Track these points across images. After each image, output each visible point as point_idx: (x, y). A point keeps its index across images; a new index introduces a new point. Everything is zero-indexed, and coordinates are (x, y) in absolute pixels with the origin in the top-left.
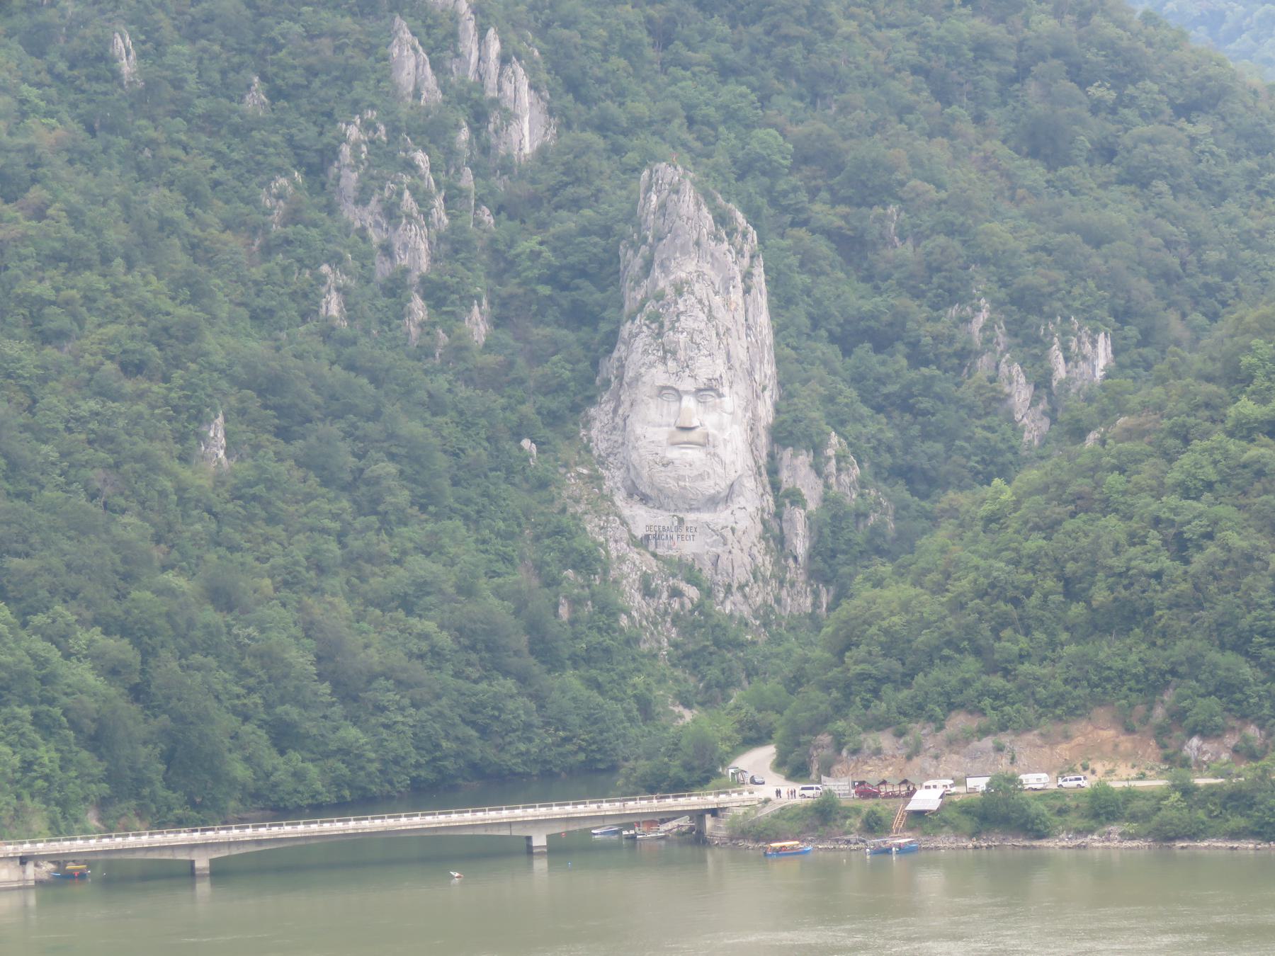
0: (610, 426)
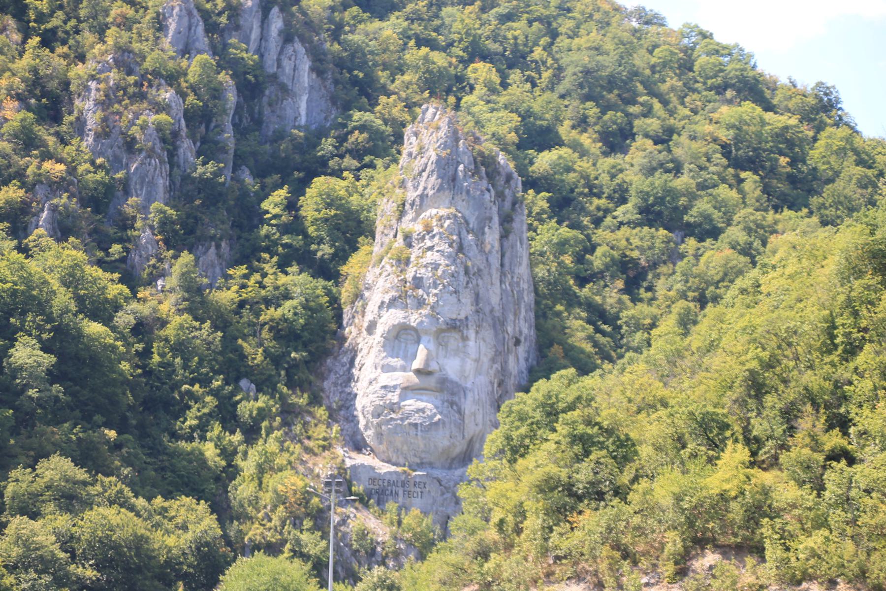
0: (345, 377)
